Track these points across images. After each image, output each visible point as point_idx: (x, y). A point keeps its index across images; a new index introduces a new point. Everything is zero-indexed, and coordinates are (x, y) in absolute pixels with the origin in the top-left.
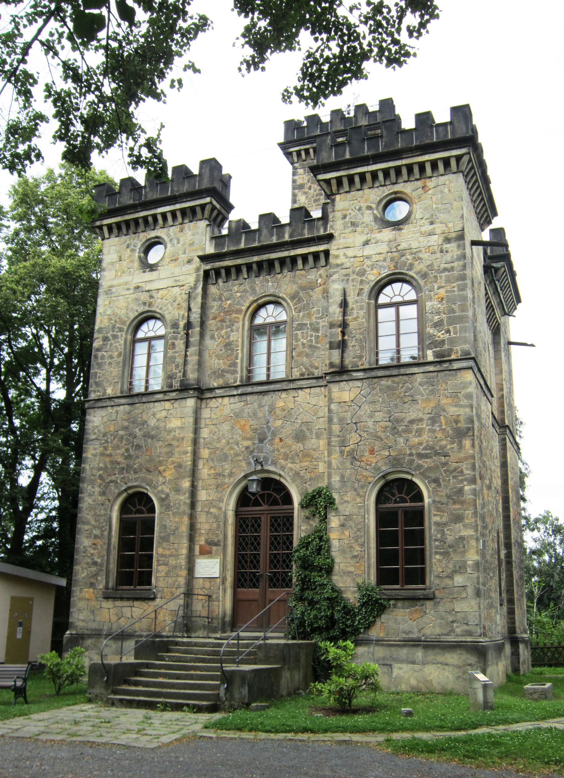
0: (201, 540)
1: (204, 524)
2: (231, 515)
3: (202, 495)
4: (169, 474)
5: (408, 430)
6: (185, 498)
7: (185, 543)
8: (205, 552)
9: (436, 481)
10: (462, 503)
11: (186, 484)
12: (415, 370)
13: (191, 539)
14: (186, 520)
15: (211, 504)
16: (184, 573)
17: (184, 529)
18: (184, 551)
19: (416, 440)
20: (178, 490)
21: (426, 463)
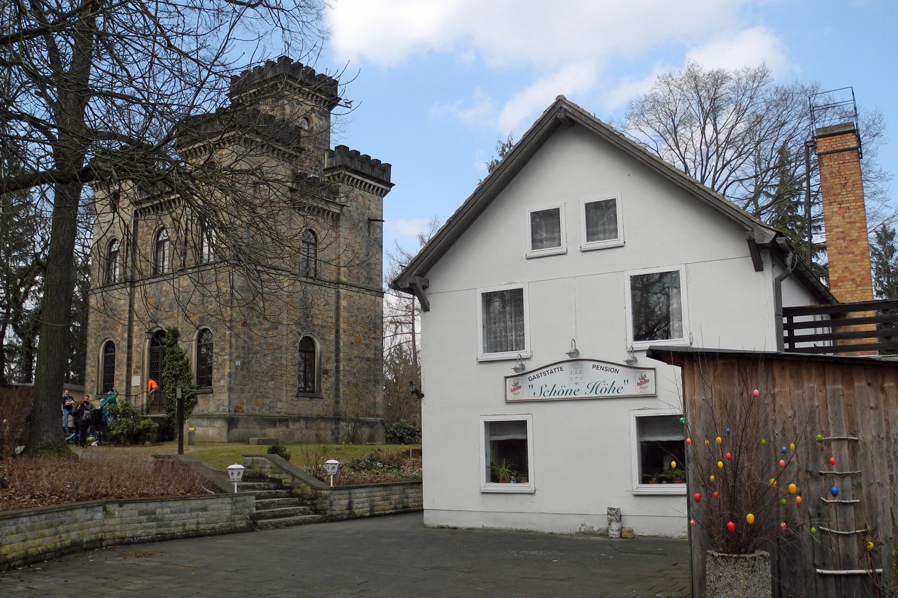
0: (134, 366)
1: (135, 357)
2: (146, 351)
3: (135, 341)
4: (120, 330)
5: (207, 302)
6: (125, 343)
7: (125, 368)
8: (136, 373)
9: (216, 330)
10: (225, 341)
11: (126, 336)
12: (209, 267)
13: (129, 365)
14: (126, 355)
15: (138, 346)
16: (125, 384)
17: (125, 360)
18: (125, 372)
19: (210, 307)
20: (123, 339)
21: (213, 320)
